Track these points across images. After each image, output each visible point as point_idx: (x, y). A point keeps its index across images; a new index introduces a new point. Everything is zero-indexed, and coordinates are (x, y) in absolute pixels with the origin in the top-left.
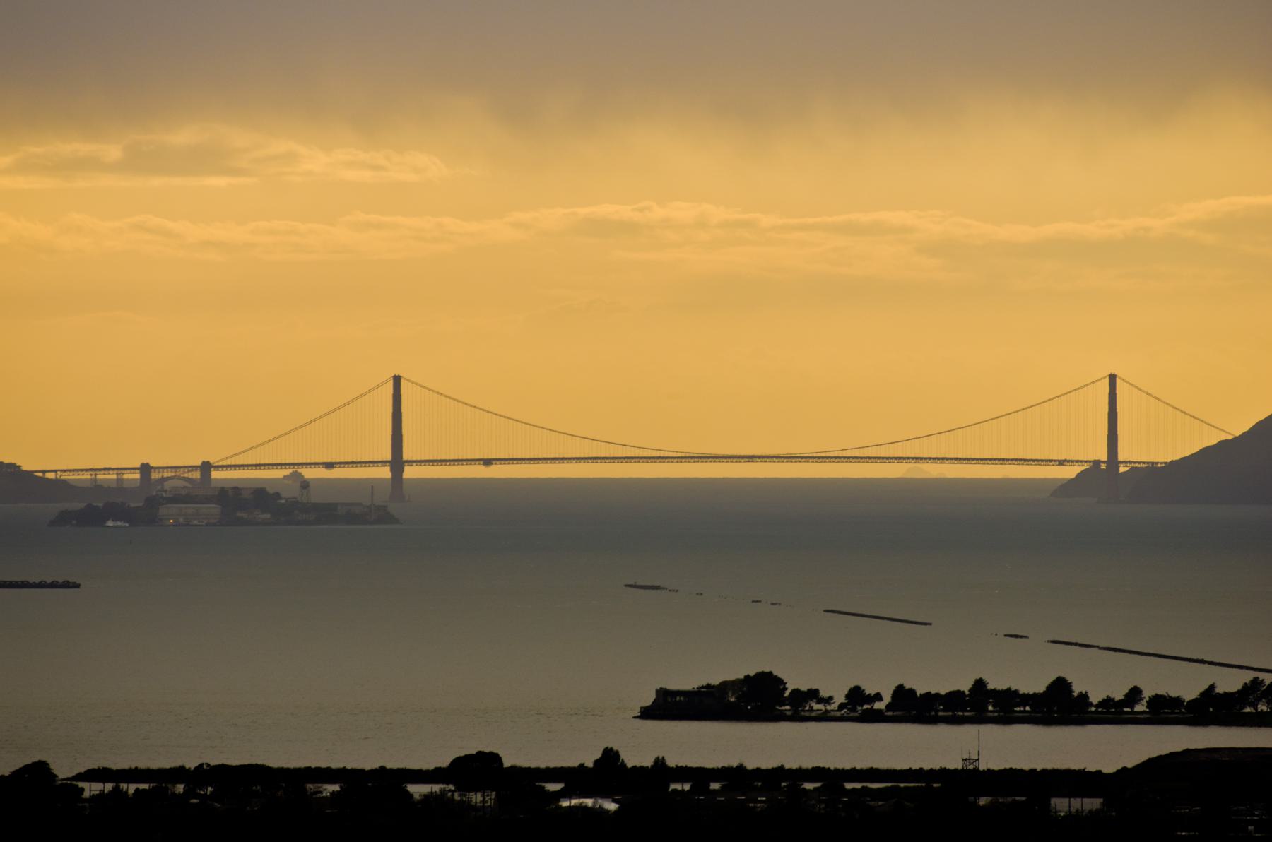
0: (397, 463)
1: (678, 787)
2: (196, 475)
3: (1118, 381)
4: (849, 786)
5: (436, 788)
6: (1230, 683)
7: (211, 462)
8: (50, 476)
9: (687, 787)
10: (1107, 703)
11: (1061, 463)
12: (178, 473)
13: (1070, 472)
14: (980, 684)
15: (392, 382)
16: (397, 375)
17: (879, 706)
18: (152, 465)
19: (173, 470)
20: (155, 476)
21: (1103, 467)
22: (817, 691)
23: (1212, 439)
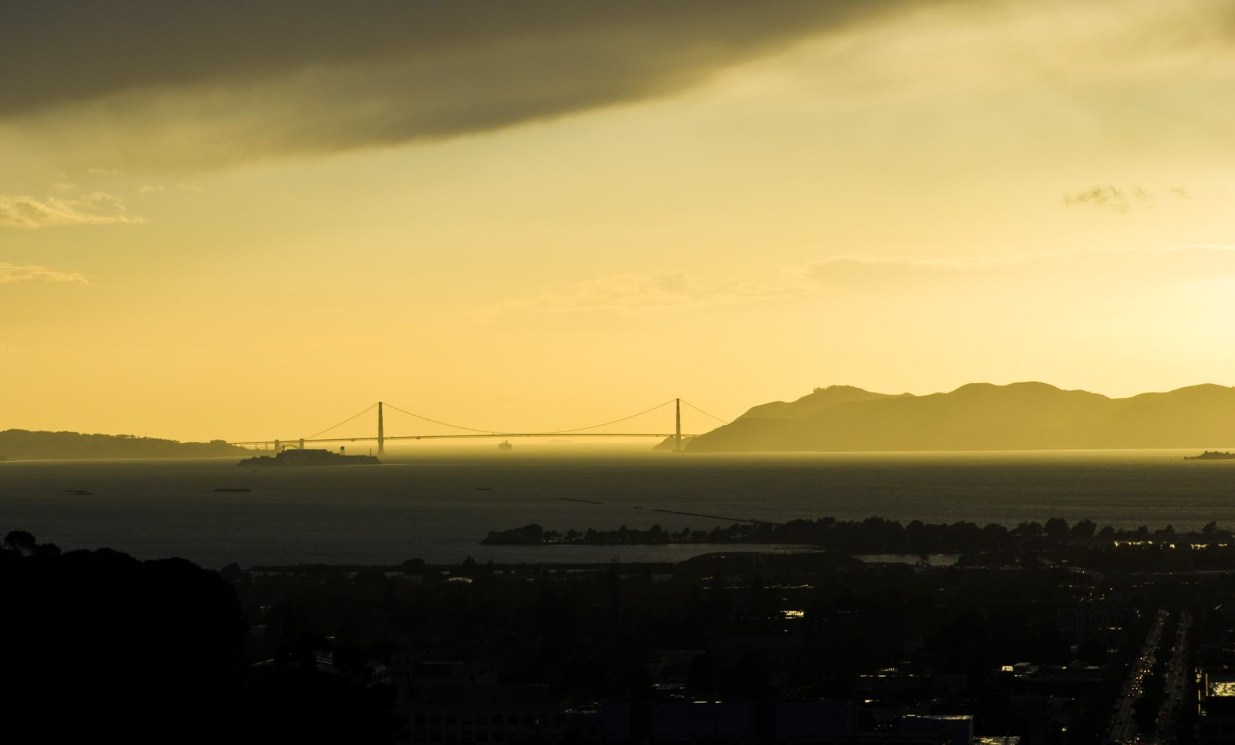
0: (381, 439)
1: (498, 572)
2: (298, 445)
3: (680, 402)
4: (569, 571)
5: (397, 574)
6: (725, 525)
7: (305, 438)
8: (238, 445)
9: (501, 572)
10: (675, 535)
11: (657, 435)
13: (661, 440)
14: (623, 528)
17: (582, 538)
21: (675, 437)
22: (555, 532)
23: (719, 425)
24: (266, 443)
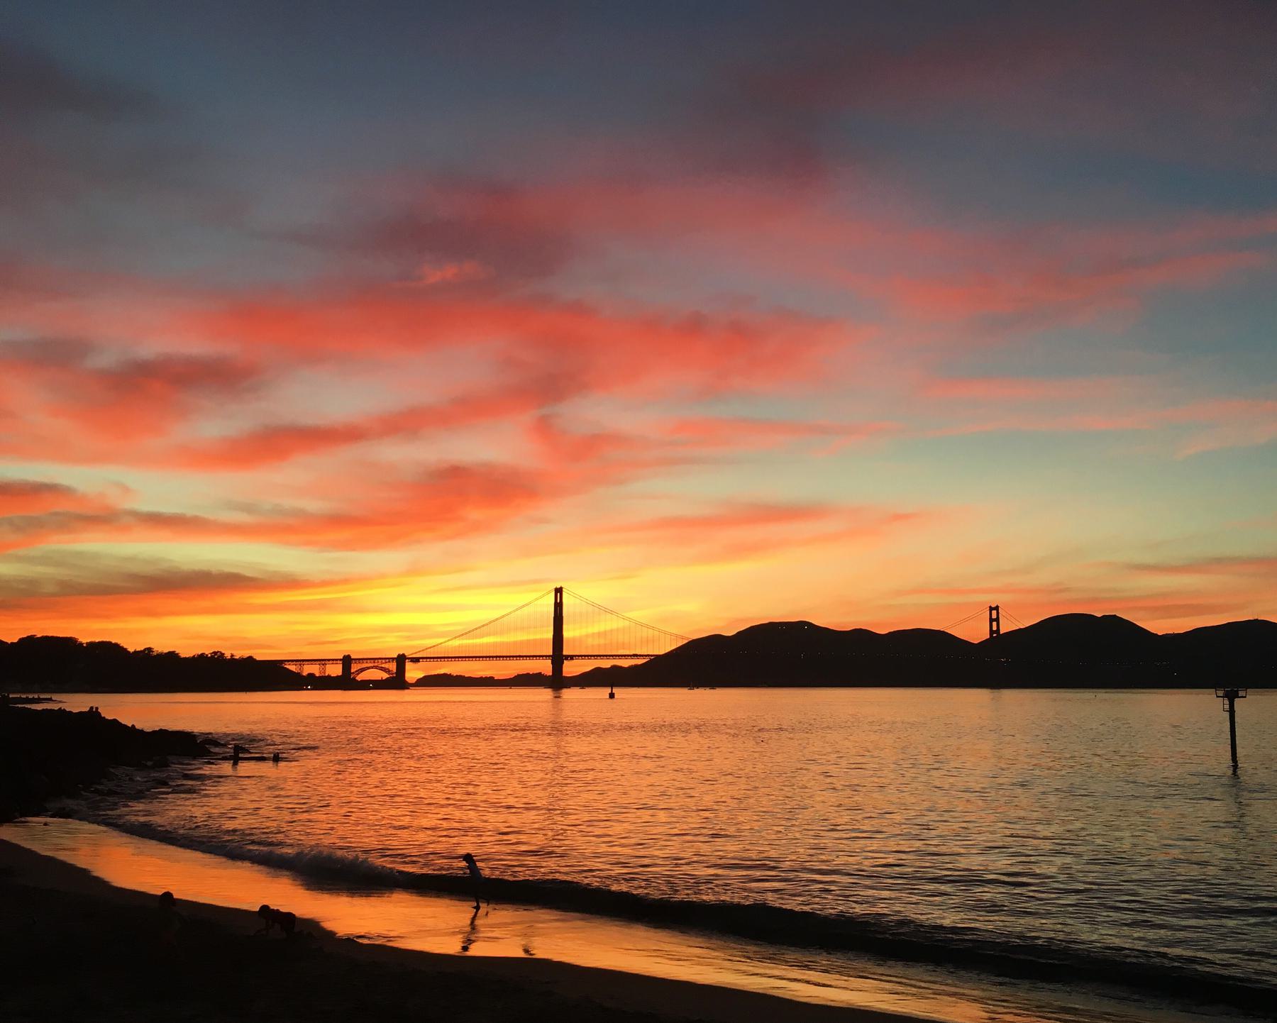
0: (558, 656)
7: (406, 654)
12: (376, 664)
16: (558, 587)
19: (372, 661)
20: (354, 668)
24: (323, 662)
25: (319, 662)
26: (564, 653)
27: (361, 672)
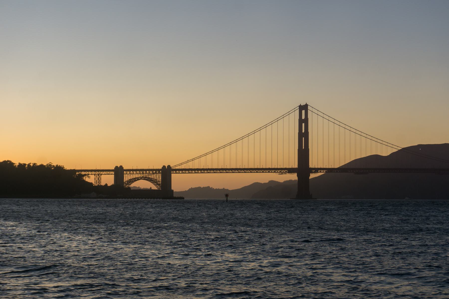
15: (298, 111)
18: (125, 168)
20: (127, 177)
24: (98, 172)
25: (94, 173)
26: (311, 166)
27: (136, 181)
